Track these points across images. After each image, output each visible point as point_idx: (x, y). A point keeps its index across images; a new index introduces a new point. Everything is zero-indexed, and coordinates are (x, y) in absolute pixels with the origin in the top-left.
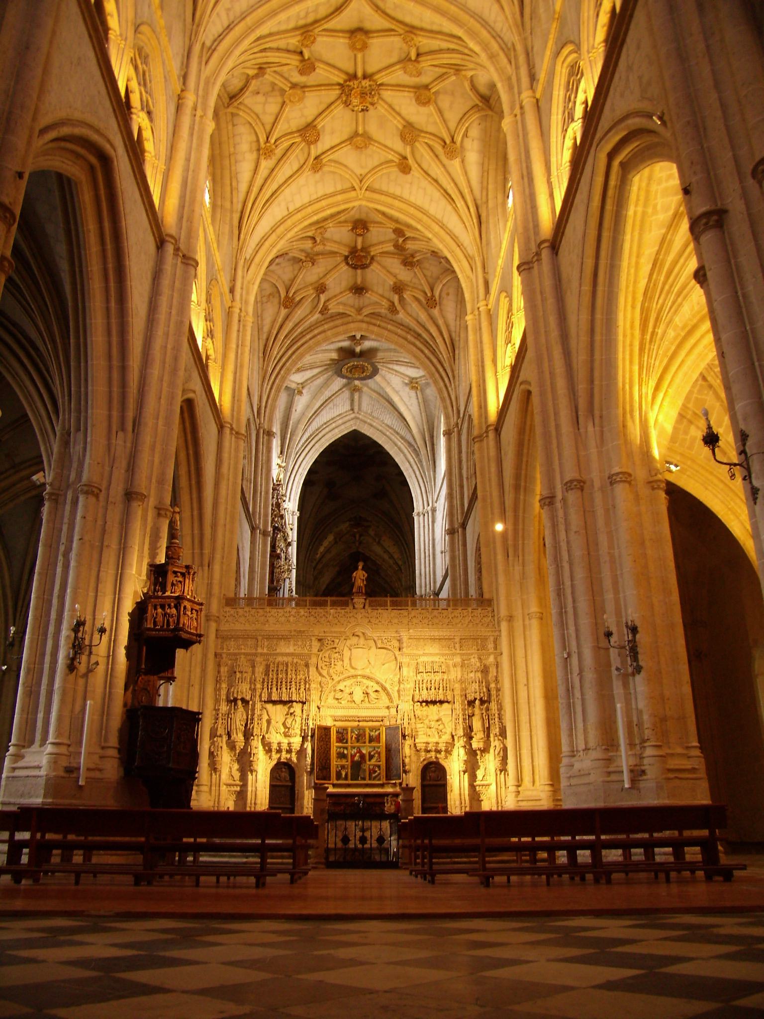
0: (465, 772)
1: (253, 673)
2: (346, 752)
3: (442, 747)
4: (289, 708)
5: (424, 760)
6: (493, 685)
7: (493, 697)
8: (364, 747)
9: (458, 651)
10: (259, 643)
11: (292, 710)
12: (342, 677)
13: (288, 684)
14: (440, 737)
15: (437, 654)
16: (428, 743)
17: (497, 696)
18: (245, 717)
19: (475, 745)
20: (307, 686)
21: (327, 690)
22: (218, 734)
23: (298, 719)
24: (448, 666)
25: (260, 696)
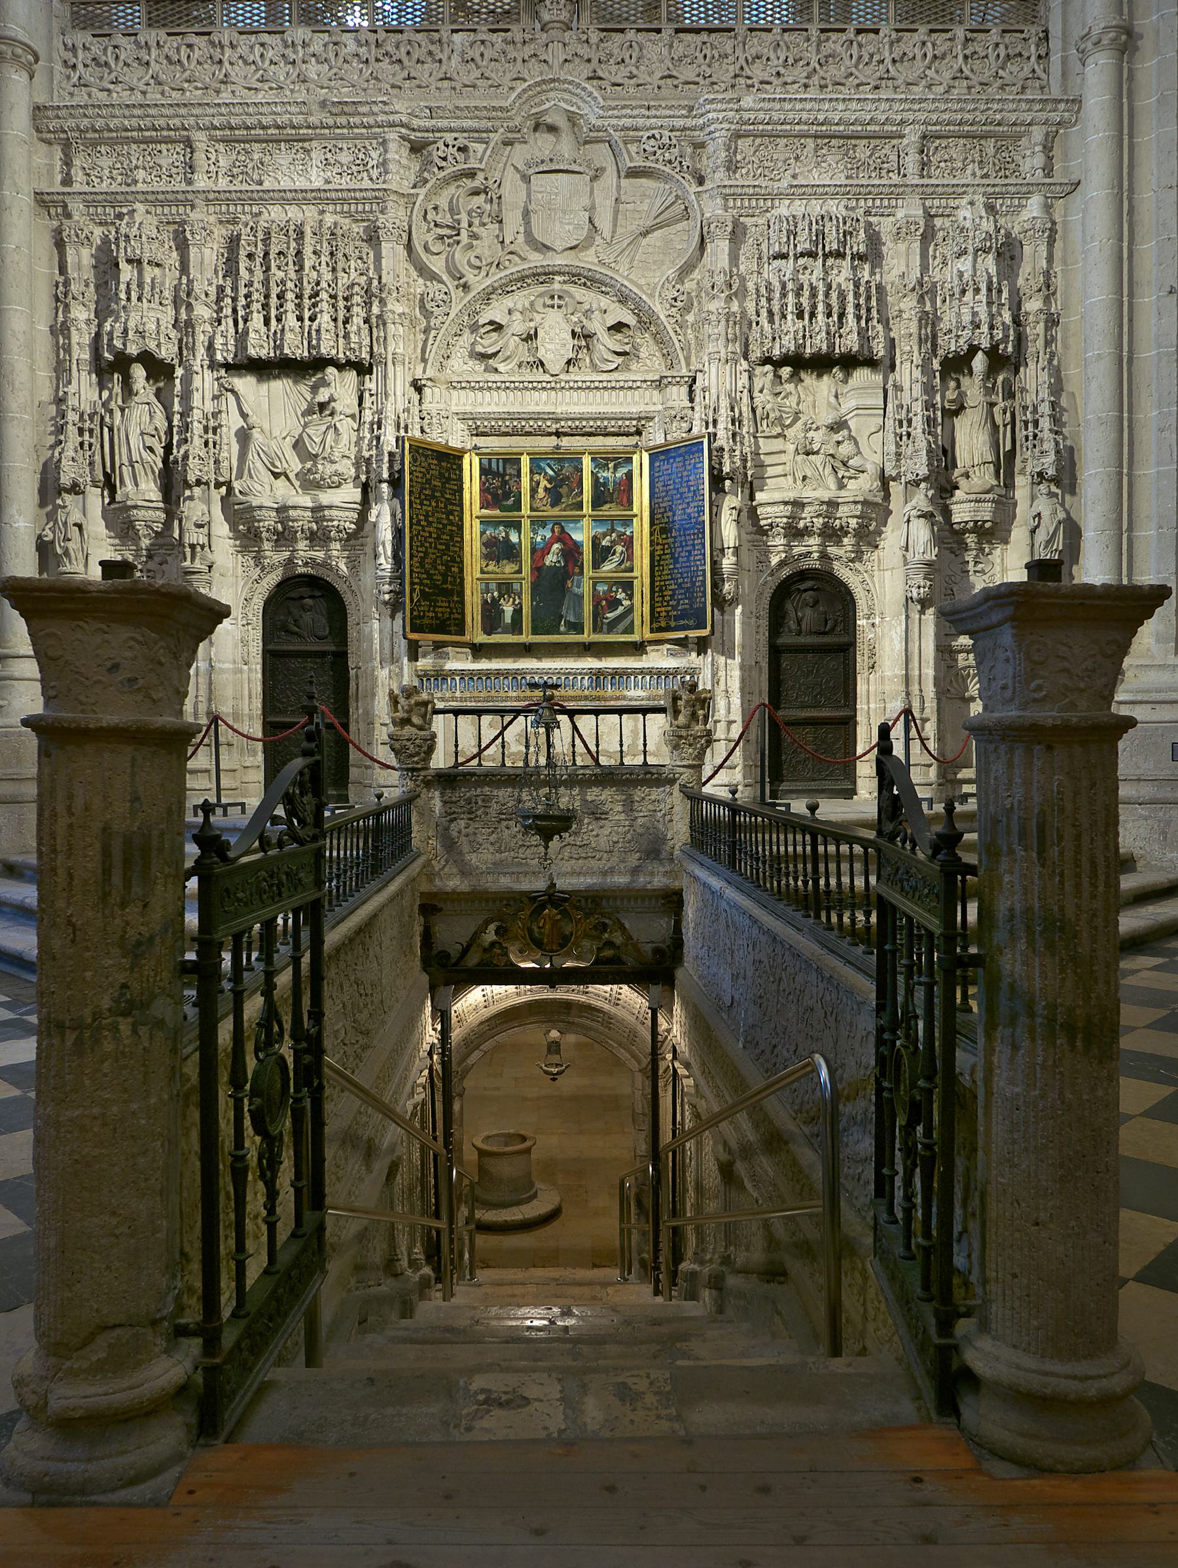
0: (924, 603)
1: (184, 268)
2: (514, 538)
3: (847, 515)
4: (315, 389)
5: (782, 564)
6: (1032, 305)
7: (1036, 345)
8: (577, 520)
9: (917, 181)
10: (200, 156)
11: (323, 395)
12: (496, 276)
13: (307, 302)
14: (841, 486)
15: (838, 192)
16: (798, 504)
17: (1047, 343)
18: (161, 422)
19: (962, 512)
20: (376, 310)
21: (445, 324)
22: (65, 480)
23: (346, 426)
24: (874, 239)
25: (210, 348)
